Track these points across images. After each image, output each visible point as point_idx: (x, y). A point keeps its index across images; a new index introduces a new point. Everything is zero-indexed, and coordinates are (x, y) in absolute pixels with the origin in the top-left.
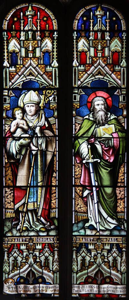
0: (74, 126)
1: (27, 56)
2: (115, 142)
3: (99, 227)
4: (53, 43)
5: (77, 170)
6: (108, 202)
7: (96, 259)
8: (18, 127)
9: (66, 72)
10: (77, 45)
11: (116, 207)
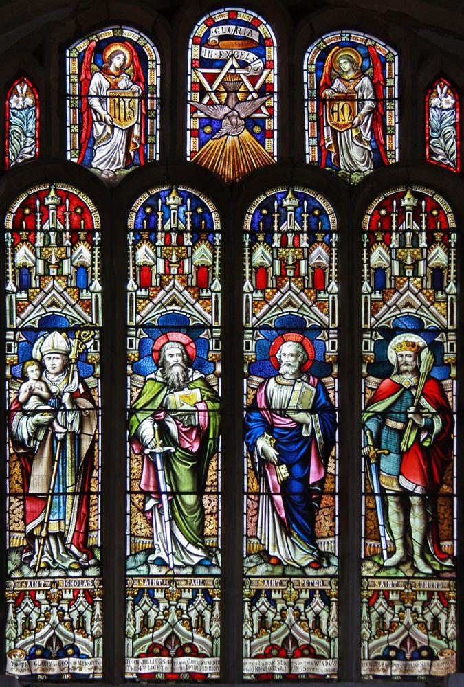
0: (129, 391)
1: (47, 274)
2: (201, 419)
3: (171, 561)
4: (92, 251)
5: (134, 466)
6: (189, 519)
7: (169, 614)
8: (31, 393)
9: (115, 300)
11: (202, 527)
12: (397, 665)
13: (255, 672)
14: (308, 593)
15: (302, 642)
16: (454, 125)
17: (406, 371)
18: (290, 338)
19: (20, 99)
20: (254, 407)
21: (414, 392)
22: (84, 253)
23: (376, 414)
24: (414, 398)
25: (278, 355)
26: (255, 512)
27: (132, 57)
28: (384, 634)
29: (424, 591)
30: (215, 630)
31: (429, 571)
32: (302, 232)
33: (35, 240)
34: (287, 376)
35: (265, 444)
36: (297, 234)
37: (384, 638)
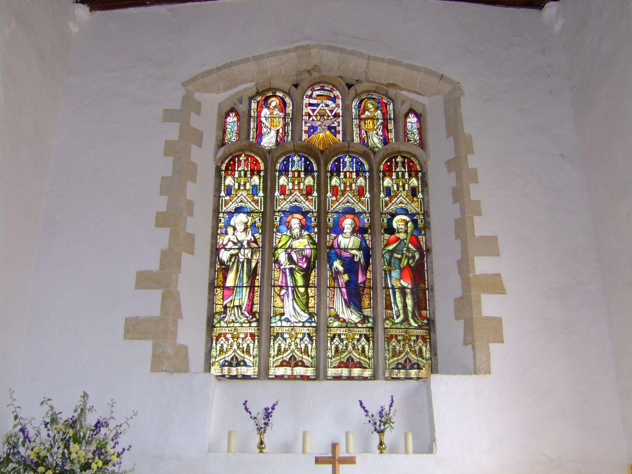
0: (274, 240)
1: (239, 188)
2: (307, 252)
3: (293, 319)
4: (260, 179)
5: (277, 274)
6: (301, 299)
7: (291, 345)
8: (229, 241)
9: (269, 199)
10: (278, 180)
11: (307, 303)
12: (403, 372)
13: (333, 375)
14: (358, 336)
15: (356, 360)
16: (417, 129)
17: (401, 232)
18: (349, 217)
19: (231, 118)
20: (332, 247)
21: (405, 241)
22: (256, 180)
23: (389, 251)
24: (405, 244)
25: (343, 224)
26: (333, 296)
27: (280, 102)
28: (396, 357)
29: (414, 335)
30: (313, 354)
31: (416, 325)
32: (353, 172)
33: (235, 175)
34: (347, 234)
35: (337, 264)
36: (351, 172)
37: (396, 359)
